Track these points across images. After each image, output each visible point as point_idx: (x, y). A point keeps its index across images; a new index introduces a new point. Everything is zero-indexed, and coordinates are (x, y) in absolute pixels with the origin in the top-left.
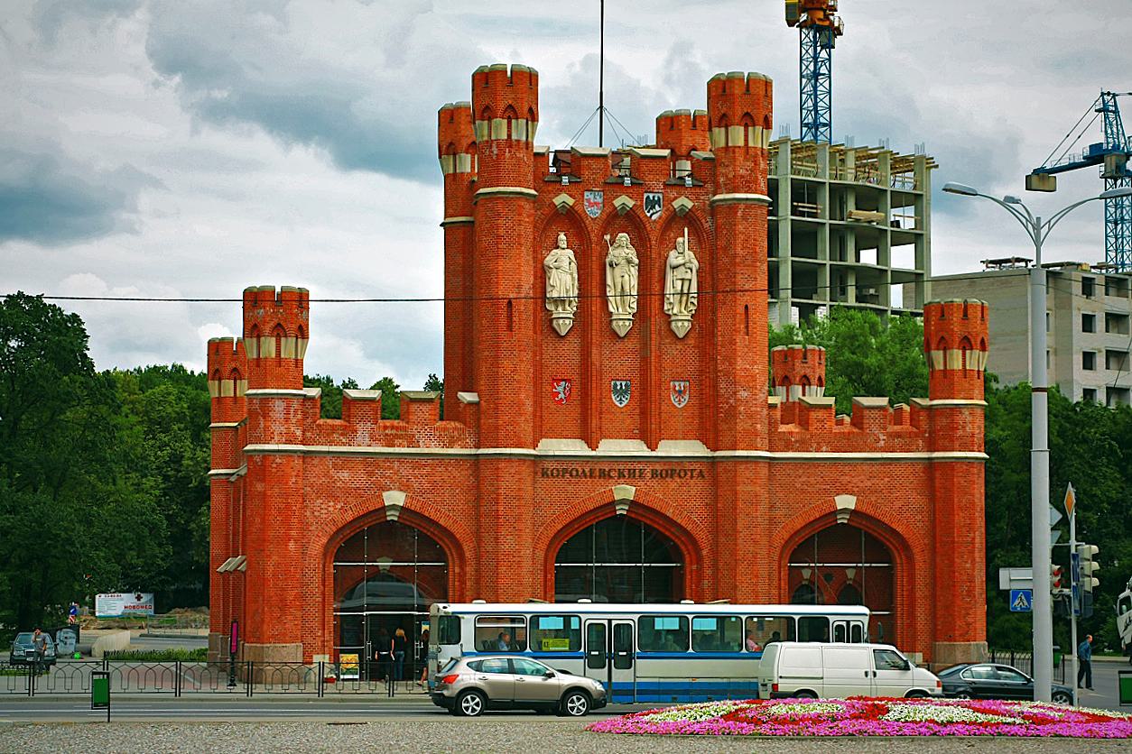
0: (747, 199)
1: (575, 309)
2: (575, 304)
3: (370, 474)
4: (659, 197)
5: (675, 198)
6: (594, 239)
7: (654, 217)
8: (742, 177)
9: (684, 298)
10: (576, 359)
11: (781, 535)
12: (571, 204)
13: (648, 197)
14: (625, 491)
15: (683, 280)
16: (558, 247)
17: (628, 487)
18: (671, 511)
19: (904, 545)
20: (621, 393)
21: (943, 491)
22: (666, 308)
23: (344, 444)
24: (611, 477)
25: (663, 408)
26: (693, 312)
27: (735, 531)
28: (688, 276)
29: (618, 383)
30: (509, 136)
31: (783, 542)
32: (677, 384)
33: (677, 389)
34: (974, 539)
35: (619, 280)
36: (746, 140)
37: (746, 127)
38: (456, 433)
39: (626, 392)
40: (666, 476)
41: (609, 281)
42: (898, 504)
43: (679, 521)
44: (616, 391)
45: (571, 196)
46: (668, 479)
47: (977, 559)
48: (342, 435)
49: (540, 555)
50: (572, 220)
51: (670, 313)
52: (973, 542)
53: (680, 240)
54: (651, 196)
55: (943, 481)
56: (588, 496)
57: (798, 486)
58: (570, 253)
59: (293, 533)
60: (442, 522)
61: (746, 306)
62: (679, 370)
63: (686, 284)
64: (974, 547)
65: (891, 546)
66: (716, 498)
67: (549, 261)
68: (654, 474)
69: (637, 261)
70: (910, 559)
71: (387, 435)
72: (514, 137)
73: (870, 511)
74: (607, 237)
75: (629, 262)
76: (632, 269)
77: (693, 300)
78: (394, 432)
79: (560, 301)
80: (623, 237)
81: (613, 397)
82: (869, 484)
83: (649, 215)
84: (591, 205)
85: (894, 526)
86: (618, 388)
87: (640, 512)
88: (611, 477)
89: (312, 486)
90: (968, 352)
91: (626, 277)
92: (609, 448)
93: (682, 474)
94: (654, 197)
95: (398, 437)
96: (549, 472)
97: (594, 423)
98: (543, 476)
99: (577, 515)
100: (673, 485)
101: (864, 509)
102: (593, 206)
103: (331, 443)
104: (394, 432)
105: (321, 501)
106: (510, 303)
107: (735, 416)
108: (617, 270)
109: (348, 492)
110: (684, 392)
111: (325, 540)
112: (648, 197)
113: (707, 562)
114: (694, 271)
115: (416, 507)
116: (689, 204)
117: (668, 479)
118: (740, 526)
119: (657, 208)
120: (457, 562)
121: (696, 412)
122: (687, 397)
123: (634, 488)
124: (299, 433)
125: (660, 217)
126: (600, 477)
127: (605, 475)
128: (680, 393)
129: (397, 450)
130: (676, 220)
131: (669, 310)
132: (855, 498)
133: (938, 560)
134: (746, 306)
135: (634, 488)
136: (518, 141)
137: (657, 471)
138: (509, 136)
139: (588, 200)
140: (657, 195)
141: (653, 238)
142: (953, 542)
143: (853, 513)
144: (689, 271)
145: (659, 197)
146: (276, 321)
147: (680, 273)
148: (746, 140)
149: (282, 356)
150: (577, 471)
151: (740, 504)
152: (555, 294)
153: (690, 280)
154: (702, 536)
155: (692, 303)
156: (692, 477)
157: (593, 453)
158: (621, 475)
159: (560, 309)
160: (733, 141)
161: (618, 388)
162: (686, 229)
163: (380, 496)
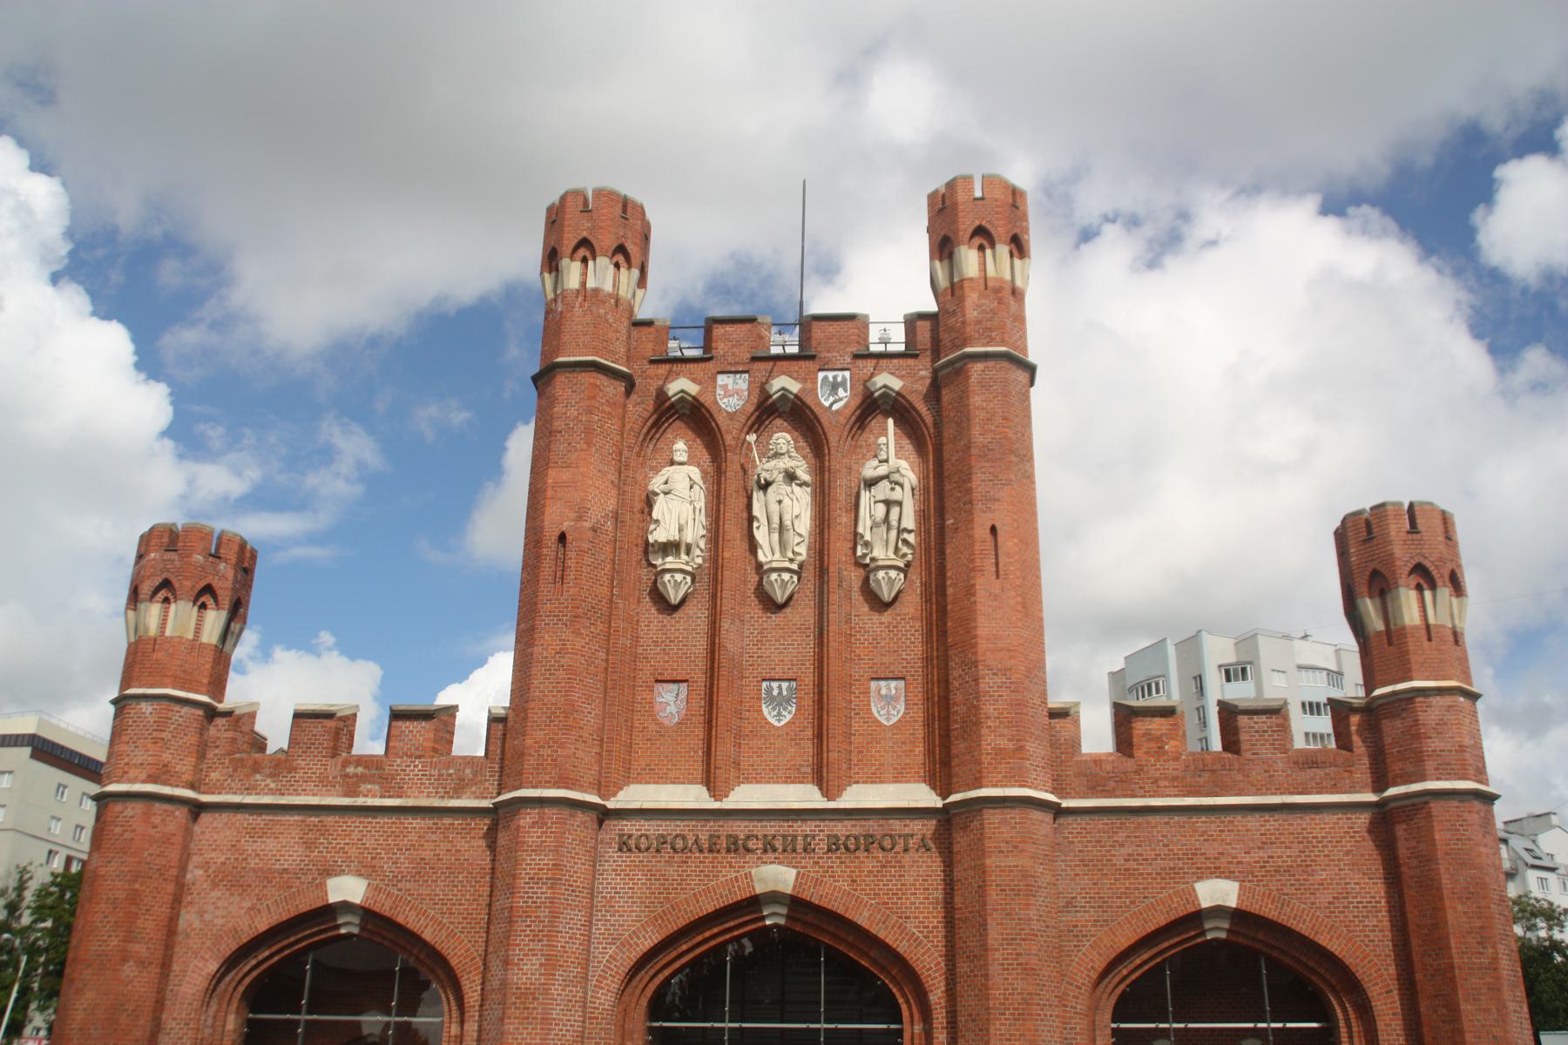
0: (986, 356)
1: (699, 561)
2: (698, 552)
3: (309, 845)
4: (844, 379)
5: (872, 375)
6: (729, 440)
7: (835, 407)
8: (979, 322)
9: (894, 533)
10: (700, 645)
11: (1089, 958)
12: (693, 393)
13: (826, 378)
14: (778, 876)
15: (888, 503)
16: (672, 463)
17: (782, 868)
18: (866, 914)
19: (1351, 985)
20: (779, 702)
21: (1415, 862)
22: (859, 553)
23: (272, 792)
24: (748, 850)
25: (855, 726)
26: (910, 557)
27: (984, 947)
28: (897, 495)
29: (775, 685)
30: (584, 284)
31: (1094, 975)
32: (883, 683)
33: (883, 692)
34: (1495, 959)
35: (774, 508)
36: (983, 265)
37: (981, 248)
38: (468, 771)
39: (788, 701)
40: (857, 849)
41: (757, 510)
42: (1324, 898)
43: (881, 935)
44: (771, 699)
45: (694, 380)
46: (861, 854)
47: (1511, 1006)
48: (271, 776)
49: (604, 998)
50: (696, 417)
51: (867, 561)
52: (1494, 967)
53: (882, 440)
54: (830, 375)
55: (1414, 843)
56: (708, 886)
57: (1119, 862)
58: (695, 473)
59: (140, 949)
60: (427, 935)
61: (993, 530)
62: (885, 659)
63: (895, 511)
64: (1498, 979)
65: (1321, 985)
66: (950, 885)
67: (656, 484)
68: (834, 845)
69: (806, 477)
70: (1364, 1009)
71: (347, 776)
72: (591, 284)
73: (1270, 911)
74: (752, 438)
75: (791, 477)
76: (797, 489)
77: (906, 536)
78: (360, 770)
79: (670, 548)
80: (783, 439)
81: (765, 710)
82: (1257, 855)
83: (827, 404)
84: (728, 394)
85: (1322, 940)
86: (775, 693)
87: (810, 918)
88: (748, 850)
89: (206, 865)
90: (1428, 594)
91: (787, 501)
92: (746, 796)
93: (887, 843)
94: (835, 378)
95: (363, 779)
96: (632, 843)
97: (724, 750)
98: (620, 850)
99: (682, 923)
100: (870, 865)
101: (1254, 908)
102: (731, 394)
103: (249, 790)
104: (360, 770)
105: (219, 894)
106: (562, 538)
107: (978, 723)
108: (770, 489)
109: (266, 876)
110: (896, 699)
111: (213, 967)
112: (826, 378)
113: (940, 1017)
114: (907, 487)
115: (384, 907)
116: (896, 384)
117: (861, 854)
118: (994, 935)
119: (841, 393)
120: (455, 1013)
121: (920, 733)
122: (901, 707)
123: (794, 871)
124: (185, 767)
125: (845, 406)
126: (728, 851)
127: (737, 847)
128: (889, 700)
129: (360, 801)
130: (871, 407)
131: (865, 555)
132: (1236, 885)
133: (1424, 1007)
134: (993, 530)
135: (794, 871)
136: (596, 291)
137: (836, 836)
138: (584, 284)
139: (725, 387)
140: (840, 374)
141: (833, 438)
142: (1452, 966)
143: (1239, 917)
144: (898, 488)
145: (844, 379)
146: (165, 575)
147: (882, 490)
148: (983, 265)
149: (168, 633)
150: (684, 838)
151: (993, 895)
152: (659, 535)
153: (900, 504)
154: (928, 960)
155: (905, 542)
156: (906, 850)
157: (717, 805)
158: (769, 847)
159: (670, 559)
160: (960, 271)
161: (775, 693)
162: (890, 421)
163: (322, 887)
